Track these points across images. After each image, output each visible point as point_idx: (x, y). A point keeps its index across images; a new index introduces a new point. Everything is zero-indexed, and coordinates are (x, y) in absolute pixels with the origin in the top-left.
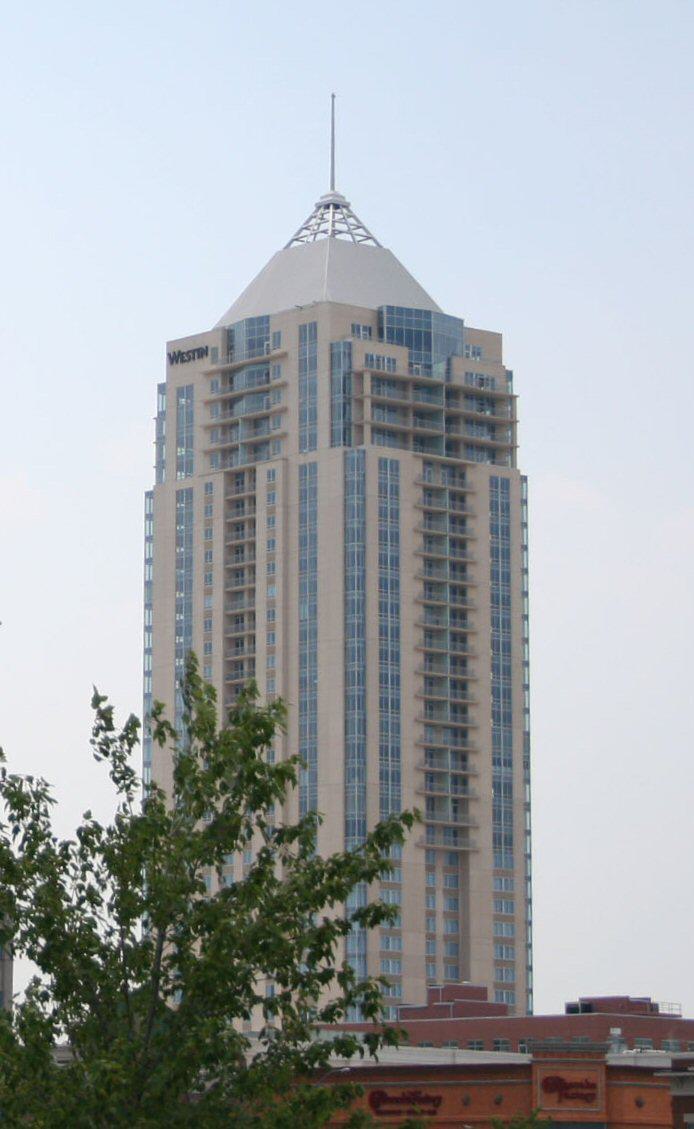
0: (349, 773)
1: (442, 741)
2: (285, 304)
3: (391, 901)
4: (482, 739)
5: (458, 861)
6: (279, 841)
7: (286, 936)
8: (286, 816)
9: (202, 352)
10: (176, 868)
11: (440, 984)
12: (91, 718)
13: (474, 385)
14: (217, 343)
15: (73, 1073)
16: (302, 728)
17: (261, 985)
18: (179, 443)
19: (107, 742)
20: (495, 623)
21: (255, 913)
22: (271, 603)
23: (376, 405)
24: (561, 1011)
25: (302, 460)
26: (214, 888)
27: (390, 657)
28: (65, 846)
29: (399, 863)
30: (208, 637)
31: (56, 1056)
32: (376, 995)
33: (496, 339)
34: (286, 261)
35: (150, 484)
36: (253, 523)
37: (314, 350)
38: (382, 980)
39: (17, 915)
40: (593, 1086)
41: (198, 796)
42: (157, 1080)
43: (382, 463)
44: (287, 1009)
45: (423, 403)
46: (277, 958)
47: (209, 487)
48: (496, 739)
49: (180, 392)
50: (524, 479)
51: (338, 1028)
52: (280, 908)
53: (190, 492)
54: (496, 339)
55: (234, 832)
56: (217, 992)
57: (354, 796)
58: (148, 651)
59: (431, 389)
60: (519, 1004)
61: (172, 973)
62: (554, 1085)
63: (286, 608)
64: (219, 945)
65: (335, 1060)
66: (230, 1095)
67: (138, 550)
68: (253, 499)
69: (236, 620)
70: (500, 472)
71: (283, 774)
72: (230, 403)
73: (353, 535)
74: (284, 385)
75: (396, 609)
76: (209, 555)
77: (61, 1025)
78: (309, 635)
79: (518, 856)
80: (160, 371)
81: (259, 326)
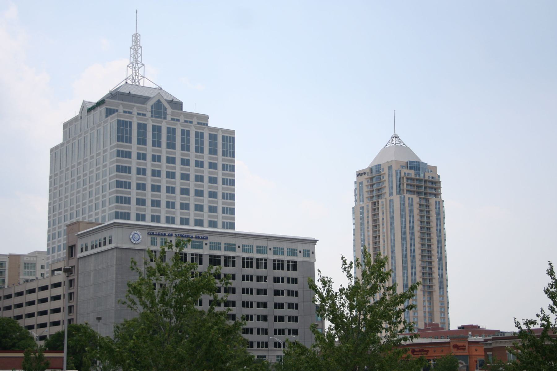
0: (404, 273)
1: (426, 265)
2: (385, 161)
3: (415, 304)
4: (435, 264)
5: (431, 293)
6: (387, 290)
7: (390, 313)
8: (389, 284)
9: (365, 173)
10: (363, 297)
11: (427, 323)
12: (341, 262)
13: (431, 179)
14: (368, 171)
15: (340, 348)
16: (392, 263)
17: (385, 325)
18: (360, 195)
19: (345, 268)
20: (437, 236)
21: (382, 308)
22: (383, 233)
23: (407, 185)
24: (457, 329)
25: (390, 198)
26: (372, 302)
27: (412, 228)
28: (336, 293)
29: (416, 294)
30: (369, 242)
31: (335, 344)
32: (412, 326)
33: (435, 168)
34: (384, 151)
35: (354, 205)
36: (378, 214)
37: (392, 172)
38: (413, 323)
39: (325, 310)
40: (465, 346)
41: (367, 280)
42: (360, 349)
43: (409, 199)
44: (391, 330)
45: (418, 184)
46: (388, 318)
47: (368, 206)
48: (439, 264)
49: (360, 183)
50: (443, 201)
51: (403, 334)
52: (388, 306)
53: (363, 207)
54: (435, 168)
55: (376, 288)
56: (374, 327)
57: (405, 279)
58: (354, 246)
59: (420, 180)
60: (447, 327)
61: (363, 323)
62: (456, 347)
63: (387, 234)
64: (374, 316)
65: (403, 342)
66: (378, 351)
67: (351, 221)
68: (378, 208)
69: (375, 237)
70: (437, 200)
71: (388, 274)
72: (372, 185)
73: (403, 216)
74: (385, 181)
75: (414, 233)
76: (368, 222)
77: (336, 336)
78: (393, 240)
79: (445, 292)
80: (355, 178)
81: (378, 167)
